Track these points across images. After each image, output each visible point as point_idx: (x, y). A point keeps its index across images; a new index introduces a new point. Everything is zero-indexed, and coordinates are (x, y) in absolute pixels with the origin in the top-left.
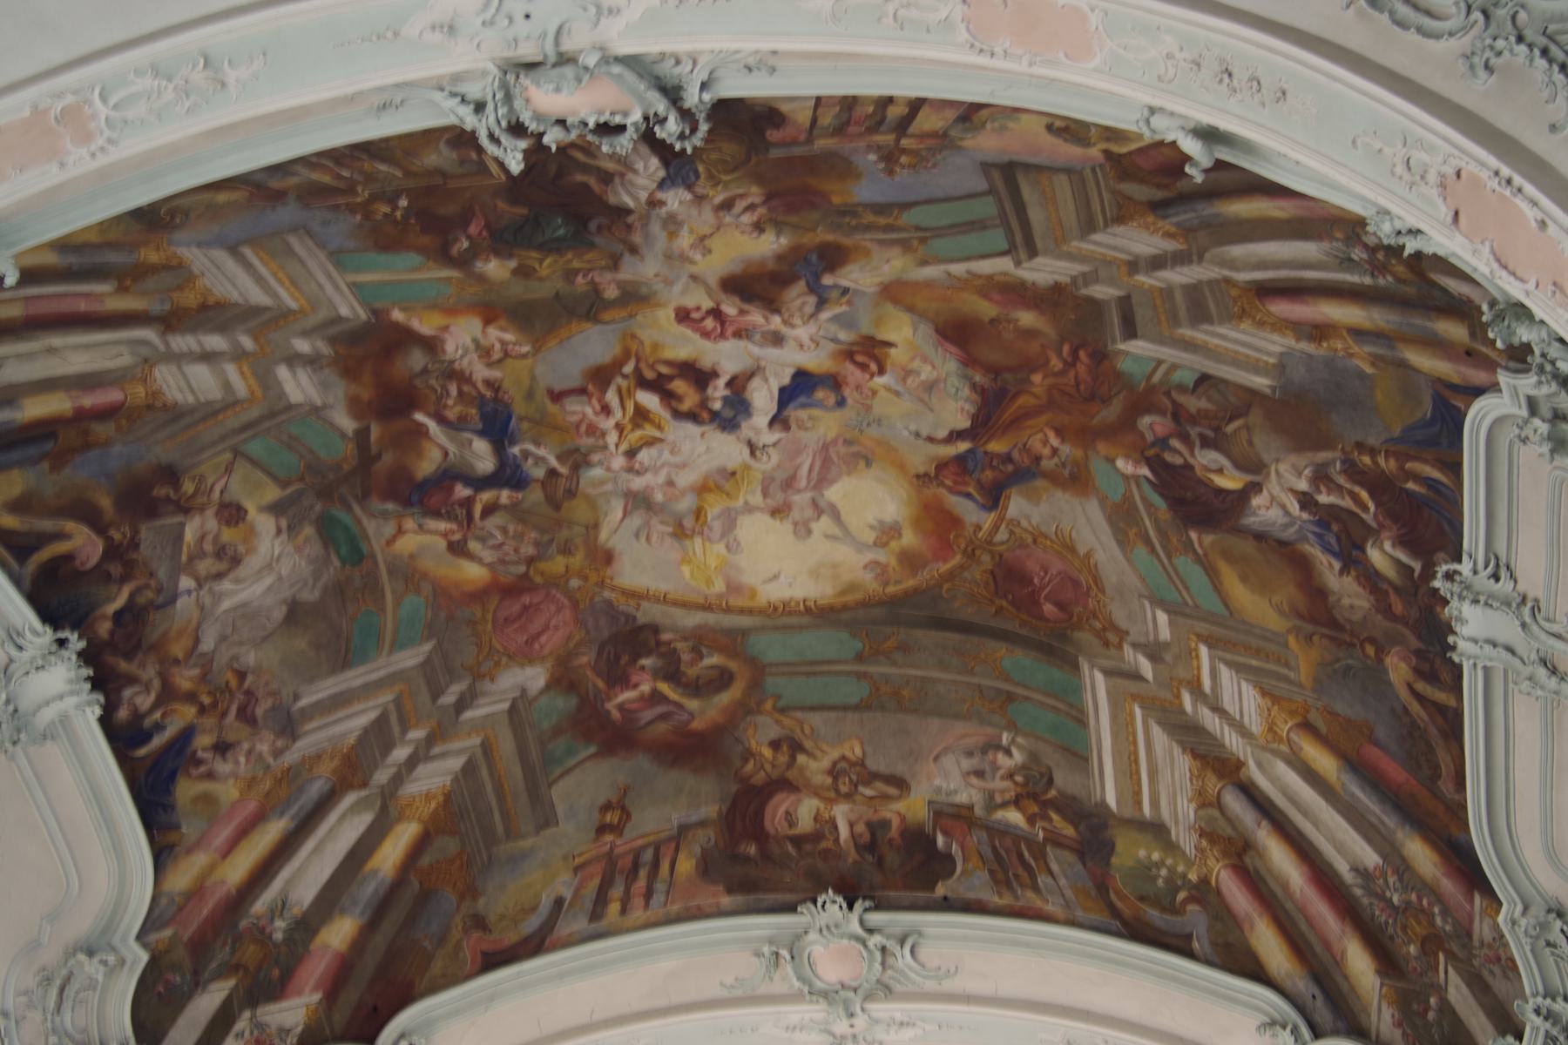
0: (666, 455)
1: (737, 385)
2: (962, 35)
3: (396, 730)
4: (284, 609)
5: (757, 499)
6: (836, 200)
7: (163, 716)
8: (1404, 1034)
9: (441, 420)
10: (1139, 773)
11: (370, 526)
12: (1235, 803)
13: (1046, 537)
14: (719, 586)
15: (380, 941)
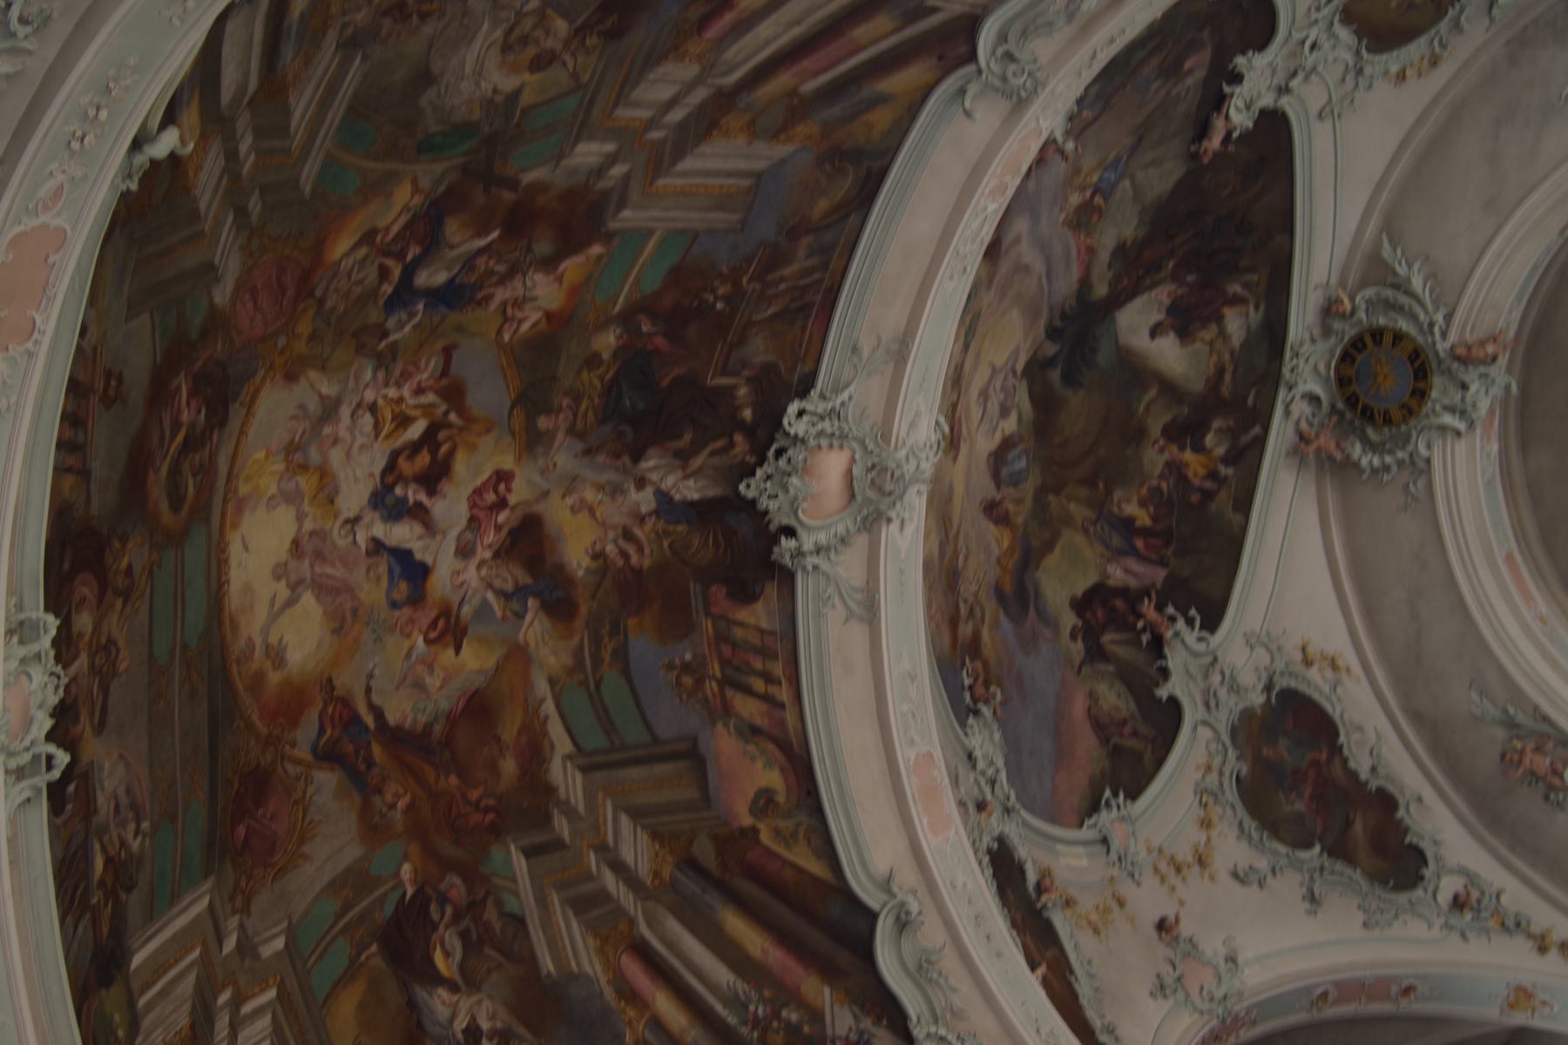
0: (360, 440)
1: (419, 513)
5: (308, 525)
6: (632, 622)
11: (439, 168)
13: (305, 812)
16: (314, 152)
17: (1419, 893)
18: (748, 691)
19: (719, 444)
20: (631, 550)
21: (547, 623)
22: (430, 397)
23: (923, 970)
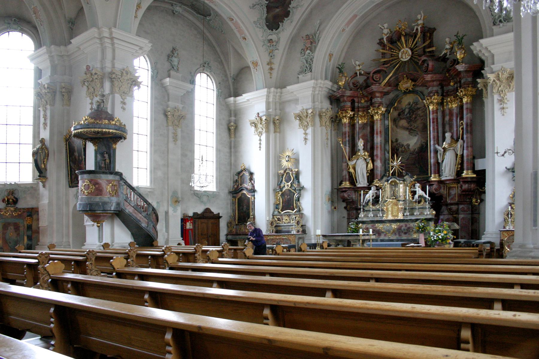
17: (269, 31)
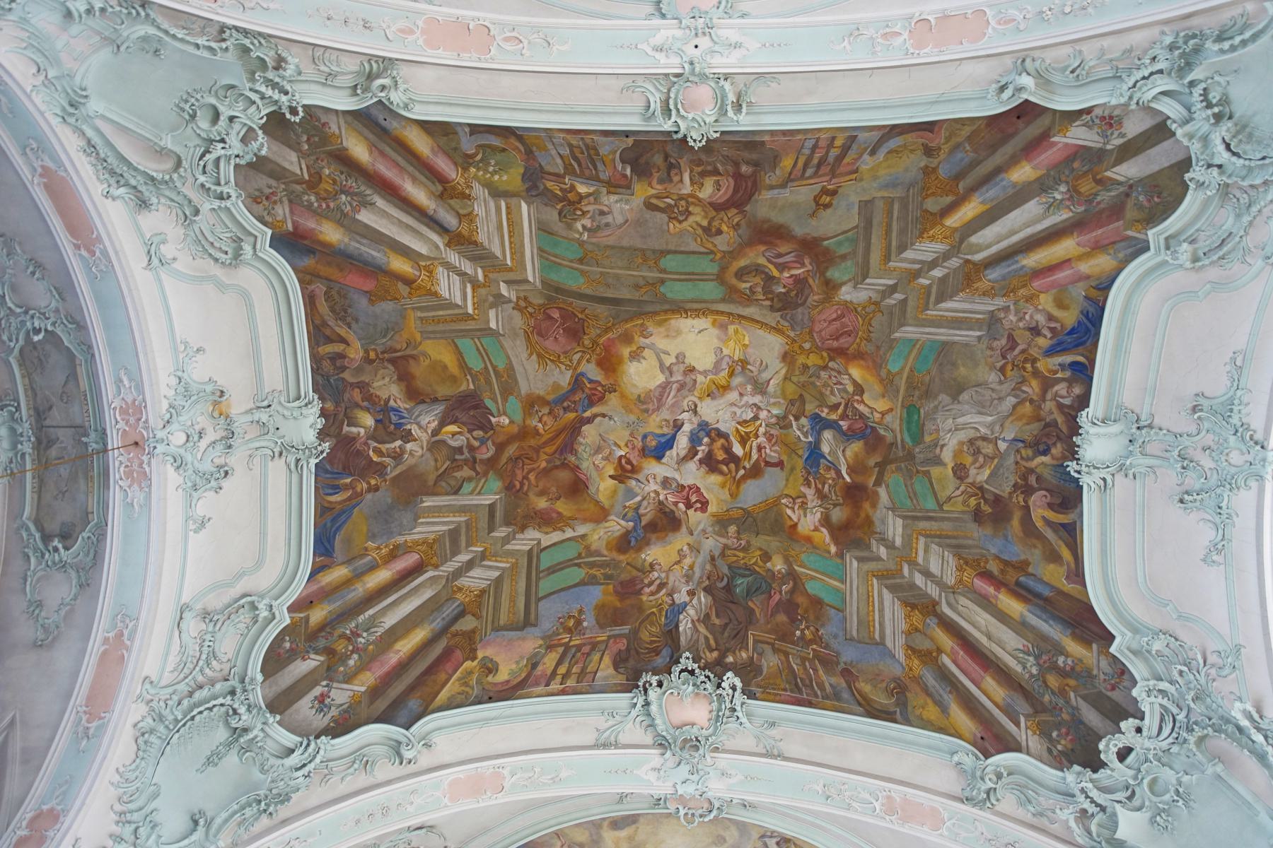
0: (739, 412)
1: (692, 453)
2: (506, 772)
3: (934, 290)
4: (961, 398)
5: (700, 378)
6: (611, 587)
7: (1056, 372)
8: (318, 120)
9: (838, 472)
10: (507, 225)
11: (896, 426)
12: (450, 220)
13: (552, 361)
14: (731, 328)
15: (998, 158)
16: (922, 330)
18: (559, 663)
19: (712, 642)
20: (653, 588)
21: (618, 534)
22: (755, 456)
23: (362, 760)
